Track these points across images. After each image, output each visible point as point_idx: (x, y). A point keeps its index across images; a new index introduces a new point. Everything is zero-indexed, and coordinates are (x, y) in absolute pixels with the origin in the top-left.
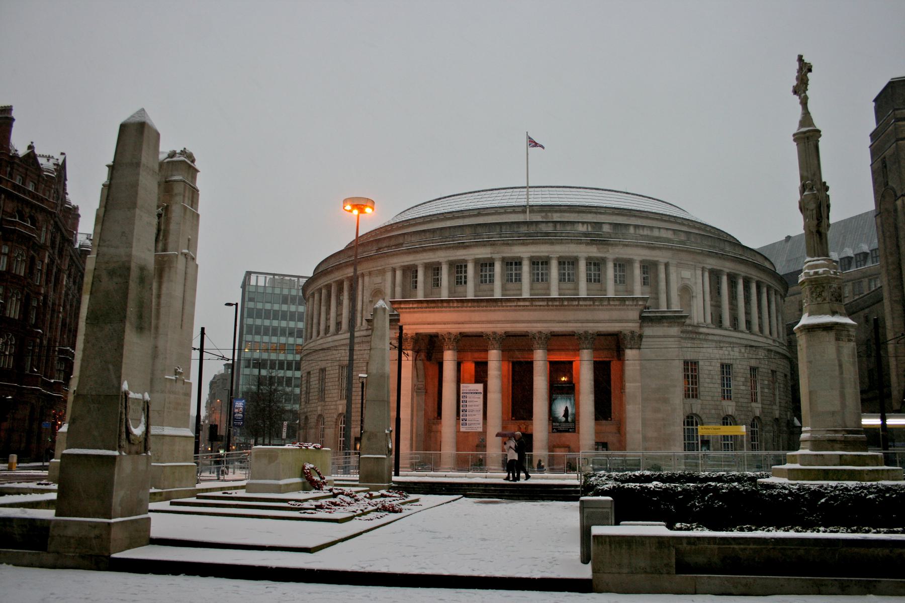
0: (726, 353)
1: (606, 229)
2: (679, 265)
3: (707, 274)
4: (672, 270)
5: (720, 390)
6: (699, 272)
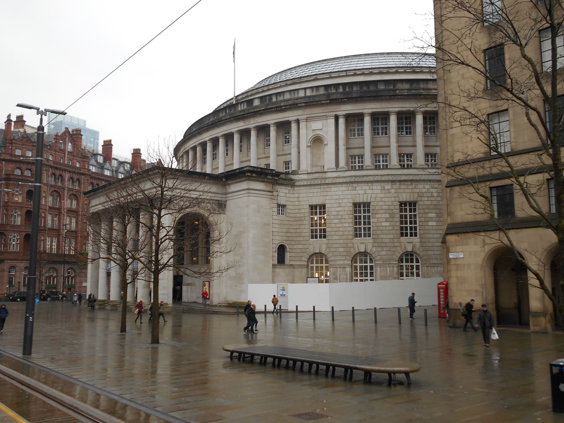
0: (363, 192)
1: (257, 103)
2: (307, 120)
3: (342, 121)
4: (302, 125)
5: (352, 229)
6: (333, 121)
